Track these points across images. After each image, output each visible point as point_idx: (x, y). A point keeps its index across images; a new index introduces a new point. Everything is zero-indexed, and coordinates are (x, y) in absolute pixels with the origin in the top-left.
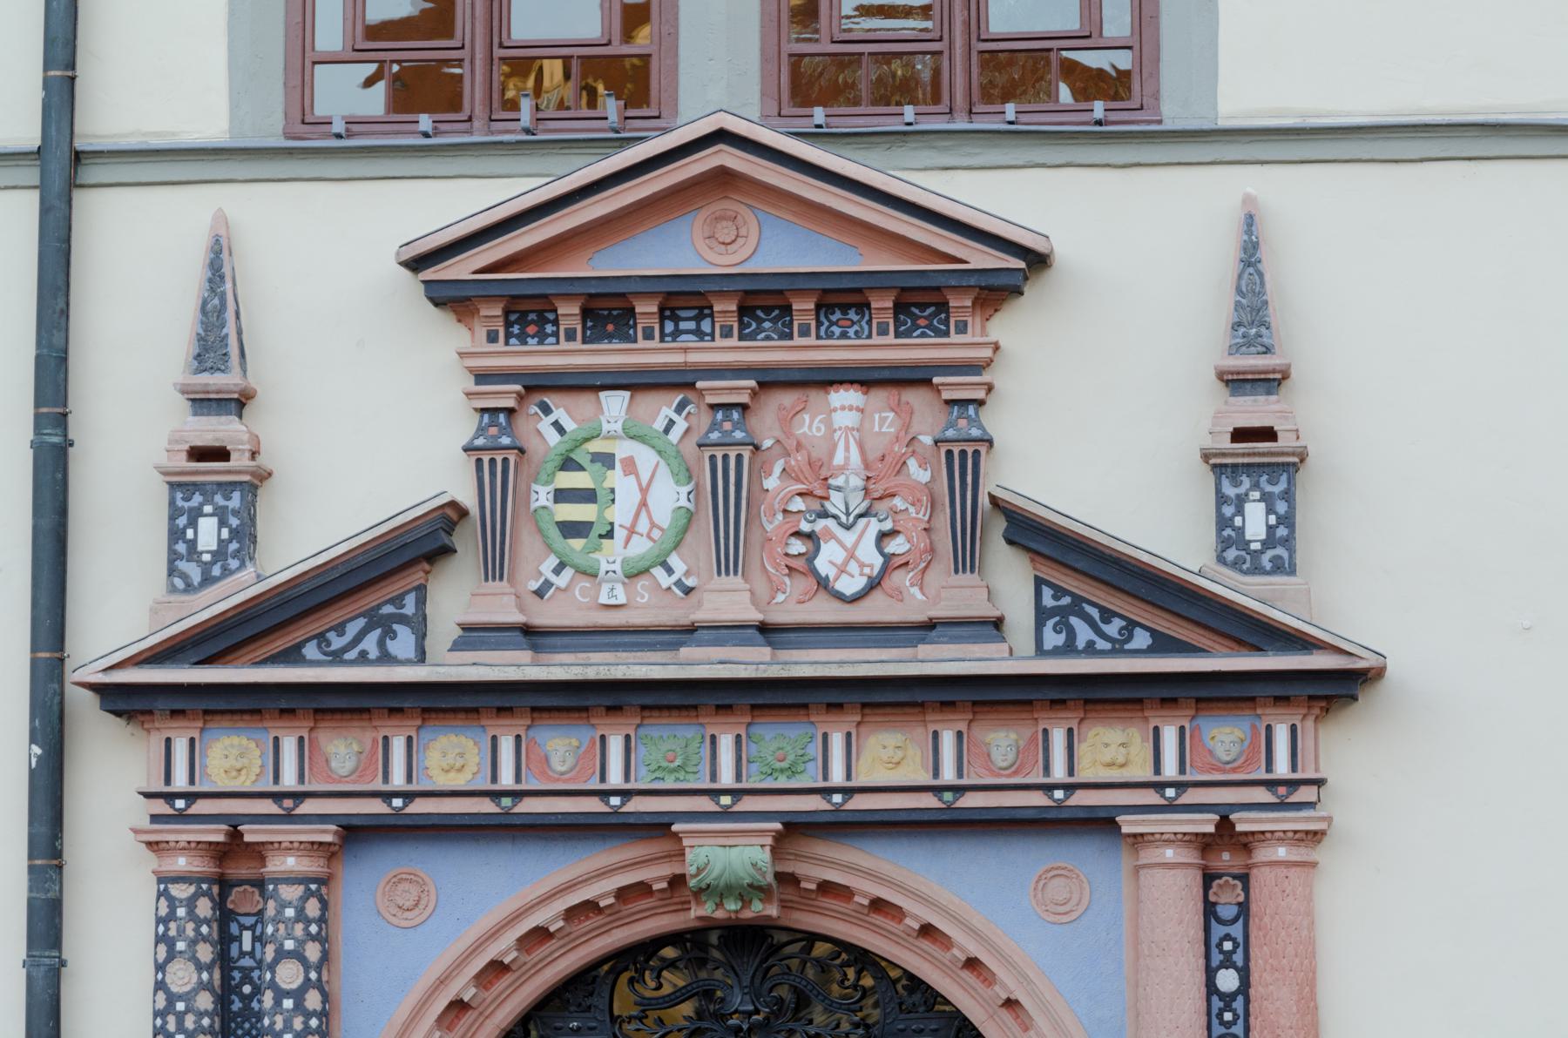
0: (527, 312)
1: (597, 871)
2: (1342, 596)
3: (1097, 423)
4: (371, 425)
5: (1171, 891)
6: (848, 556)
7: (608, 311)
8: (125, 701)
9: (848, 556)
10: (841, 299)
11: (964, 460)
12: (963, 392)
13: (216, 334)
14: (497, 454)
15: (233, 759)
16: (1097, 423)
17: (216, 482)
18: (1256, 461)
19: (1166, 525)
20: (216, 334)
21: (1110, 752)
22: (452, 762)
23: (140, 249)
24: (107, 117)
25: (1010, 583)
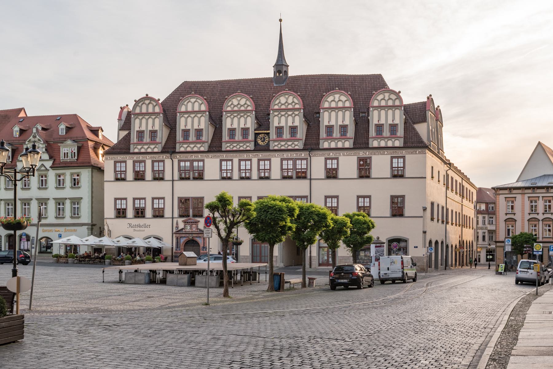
11: (197, 227)
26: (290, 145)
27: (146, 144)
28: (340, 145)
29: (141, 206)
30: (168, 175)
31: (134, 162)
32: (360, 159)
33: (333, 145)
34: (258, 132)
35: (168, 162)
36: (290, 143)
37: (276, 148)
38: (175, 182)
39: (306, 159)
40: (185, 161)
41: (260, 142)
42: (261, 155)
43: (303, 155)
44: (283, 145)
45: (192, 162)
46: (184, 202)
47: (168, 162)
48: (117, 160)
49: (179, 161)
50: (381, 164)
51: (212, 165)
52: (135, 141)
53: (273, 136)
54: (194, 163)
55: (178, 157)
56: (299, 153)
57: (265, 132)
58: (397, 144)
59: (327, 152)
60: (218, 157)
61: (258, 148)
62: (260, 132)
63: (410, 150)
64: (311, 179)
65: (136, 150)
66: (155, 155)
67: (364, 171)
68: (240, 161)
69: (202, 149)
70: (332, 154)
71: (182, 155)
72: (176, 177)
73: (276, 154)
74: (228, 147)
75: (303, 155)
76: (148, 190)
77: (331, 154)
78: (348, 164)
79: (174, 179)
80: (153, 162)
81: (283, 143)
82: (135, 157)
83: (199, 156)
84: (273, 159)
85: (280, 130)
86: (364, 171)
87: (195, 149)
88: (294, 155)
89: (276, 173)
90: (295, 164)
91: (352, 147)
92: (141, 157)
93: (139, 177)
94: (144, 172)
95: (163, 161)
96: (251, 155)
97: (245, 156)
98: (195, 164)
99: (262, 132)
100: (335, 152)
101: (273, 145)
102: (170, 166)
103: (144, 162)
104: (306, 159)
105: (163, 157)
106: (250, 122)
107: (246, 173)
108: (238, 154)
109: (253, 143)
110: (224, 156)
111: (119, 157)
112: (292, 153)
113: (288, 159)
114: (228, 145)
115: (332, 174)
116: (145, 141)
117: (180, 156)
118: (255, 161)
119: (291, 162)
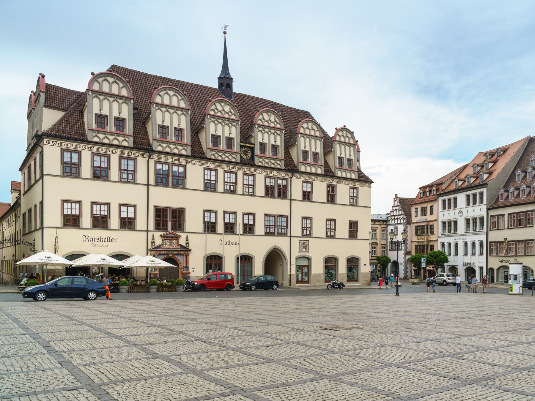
0: (164, 237)
1: (165, 256)
2: (190, 248)
3: (182, 242)
4: (158, 241)
5: (185, 257)
6: (174, 246)
7: (167, 237)
8: (151, 250)
9: (174, 246)
10: (175, 237)
12: (178, 241)
13: (153, 237)
14: (163, 242)
15: (154, 252)
16: (182, 242)
17: (153, 243)
18: (187, 243)
19: (185, 245)
20: (153, 237)
21: (183, 253)
22: (162, 252)
23: (150, 234)
24: (149, 229)
25: (179, 247)
26: (272, 164)
27: (111, 133)
28: (314, 170)
29: (102, 213)
30: (141, 177)
31: (94, 154)
32: (328, 186)
33: (308, 170)
34: (243, 144)
35: (142, 162)
36: (273, 162)
37: (260, 164)
38: (150, 187)
39: (287, 180)
40: (162, 163)
41: (243, 155)
42: (247, 169)
43: (284, 175)
44: (266, 162)
45: (170, 165)
46: (160, 212)
47: (142, 162)
48: (65, 147)
49: (156, 162)
50: (343, 191)
51: (195, 173)
52: (94, 126)
53: (257, 152)
54: (174, 167)
55: (155, 157)
56: (281, 173)
57: (250, 145)
58: (353, 176)
59: (304, 175)
60: (201, 165)
61: (243, 163)
62: (245, 144)
63: (362, 184)
64: (291, 200)
65: (96, 139)
66: (124, 151)
67: (331, 198)
68: (225, 172)
69: (183, 152)
70: (308, 178)
71: (160, 156)
72: (152, 181)
73: (261, 170)
74: (213, 155)
75: (284, 175)
76: (114, 194)
77: (307, 178)
78: (320, 189)
79: (150, 183)
80: (121, 158)
81: (267, 161)
82: (95, 149)
83: (181, 161)
84: (258, 176)
85: (263, 146)
86: (331, 198)
87: (176, 151)
88: (277, 174)
89: (260, 190)
90: (276, 182)
91: (323, 173)
92: (104, 150)
93: (100, 174)
94: (108, 168)
95: (135, 160)
96: (236, 168)
97: (230, 168)
98: (175, 169)
99: (247, 145)
100: (310, 176)
101: (258, 161)
102: (144, 167)
103: (108, 157)
104: (287, 180)
105: (135, 154)
106: (234, 132)
107: (230, 186)
108: (223, 165)
109: (238, 155)
110: (209, 165)
111: (70, 145)
112: (275, 172)
113: (270, 178)
114: (213, 153)
115: (307, 196)
116: (108, 129)
117: (157, 156)
118: (240, 174)
119: (273, 181)
